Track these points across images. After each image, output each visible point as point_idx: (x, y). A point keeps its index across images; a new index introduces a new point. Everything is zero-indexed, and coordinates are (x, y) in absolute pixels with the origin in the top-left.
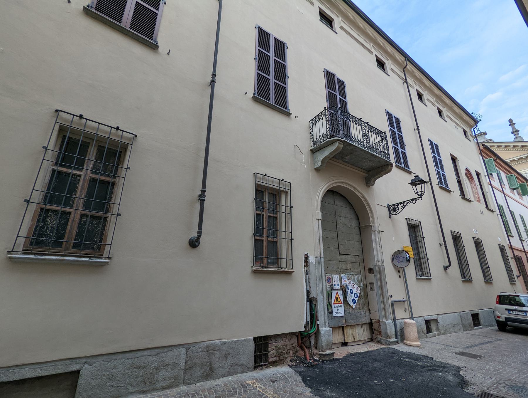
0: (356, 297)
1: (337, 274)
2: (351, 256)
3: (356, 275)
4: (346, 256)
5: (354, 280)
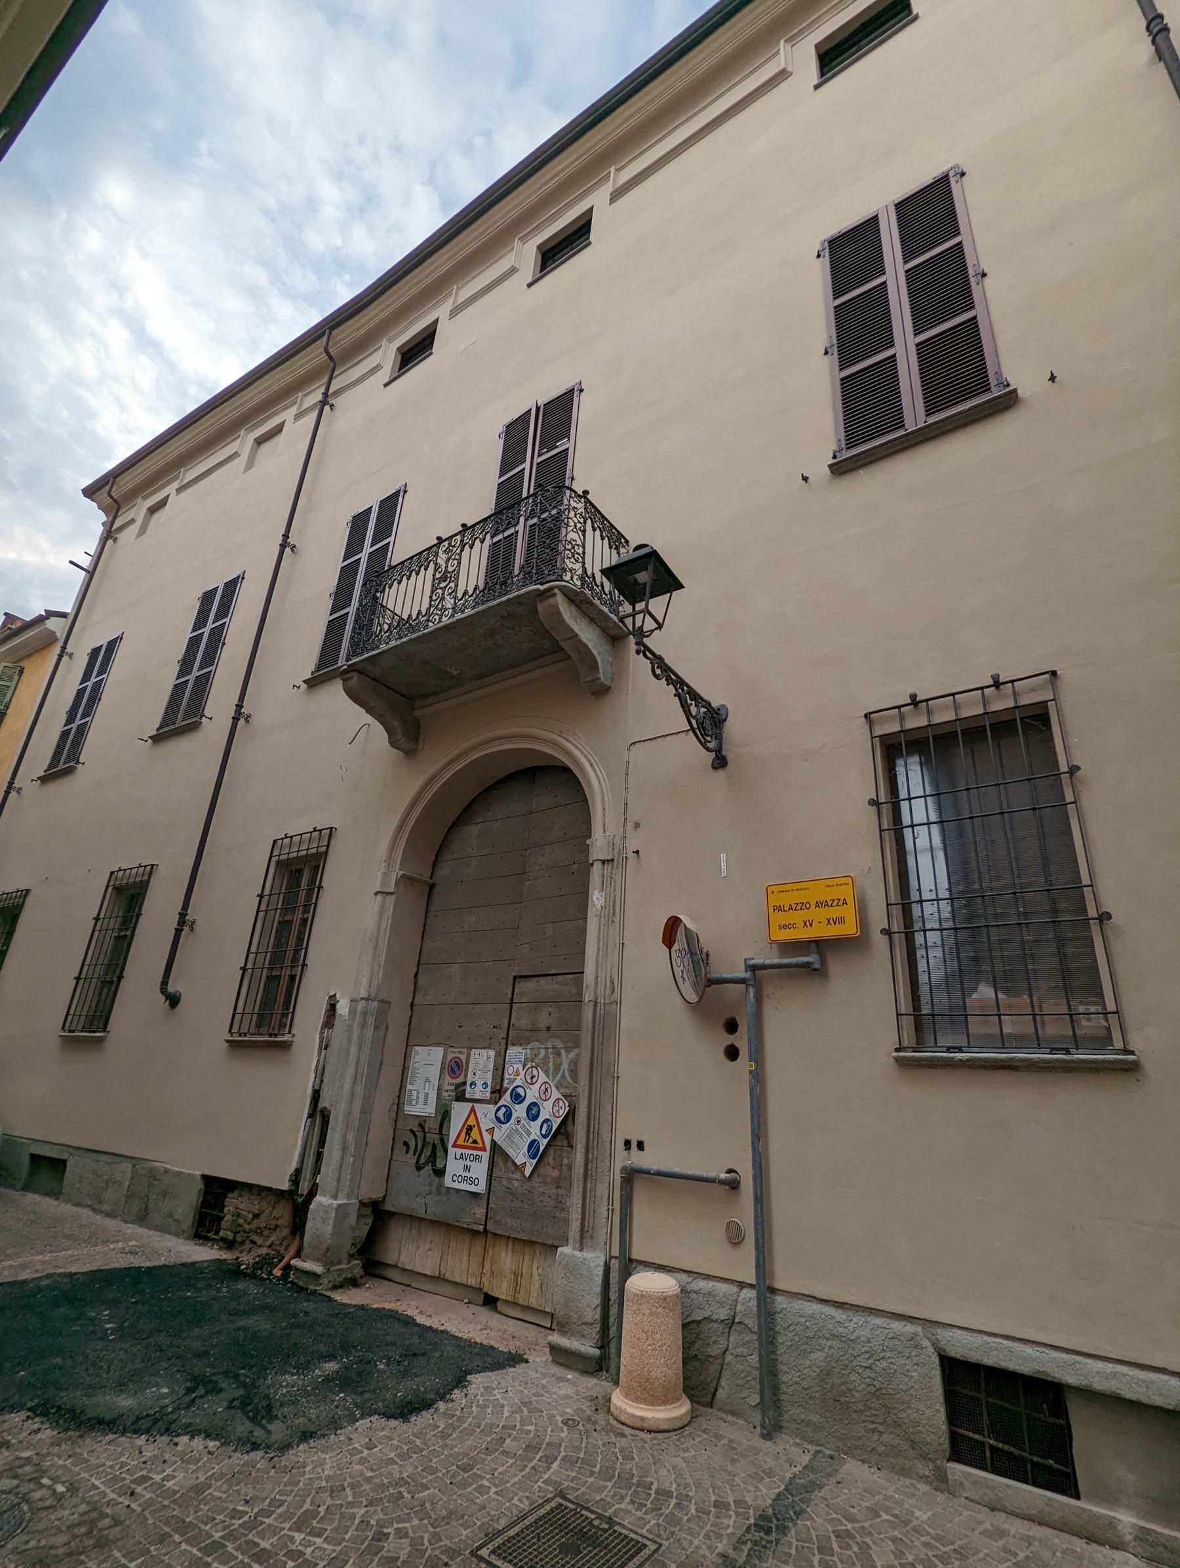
0: (545, 1136)
1: (489, 1047)
2: (560, 978)
3: (568, 1049)
4: (542, 981)
5: (557, 1067)
